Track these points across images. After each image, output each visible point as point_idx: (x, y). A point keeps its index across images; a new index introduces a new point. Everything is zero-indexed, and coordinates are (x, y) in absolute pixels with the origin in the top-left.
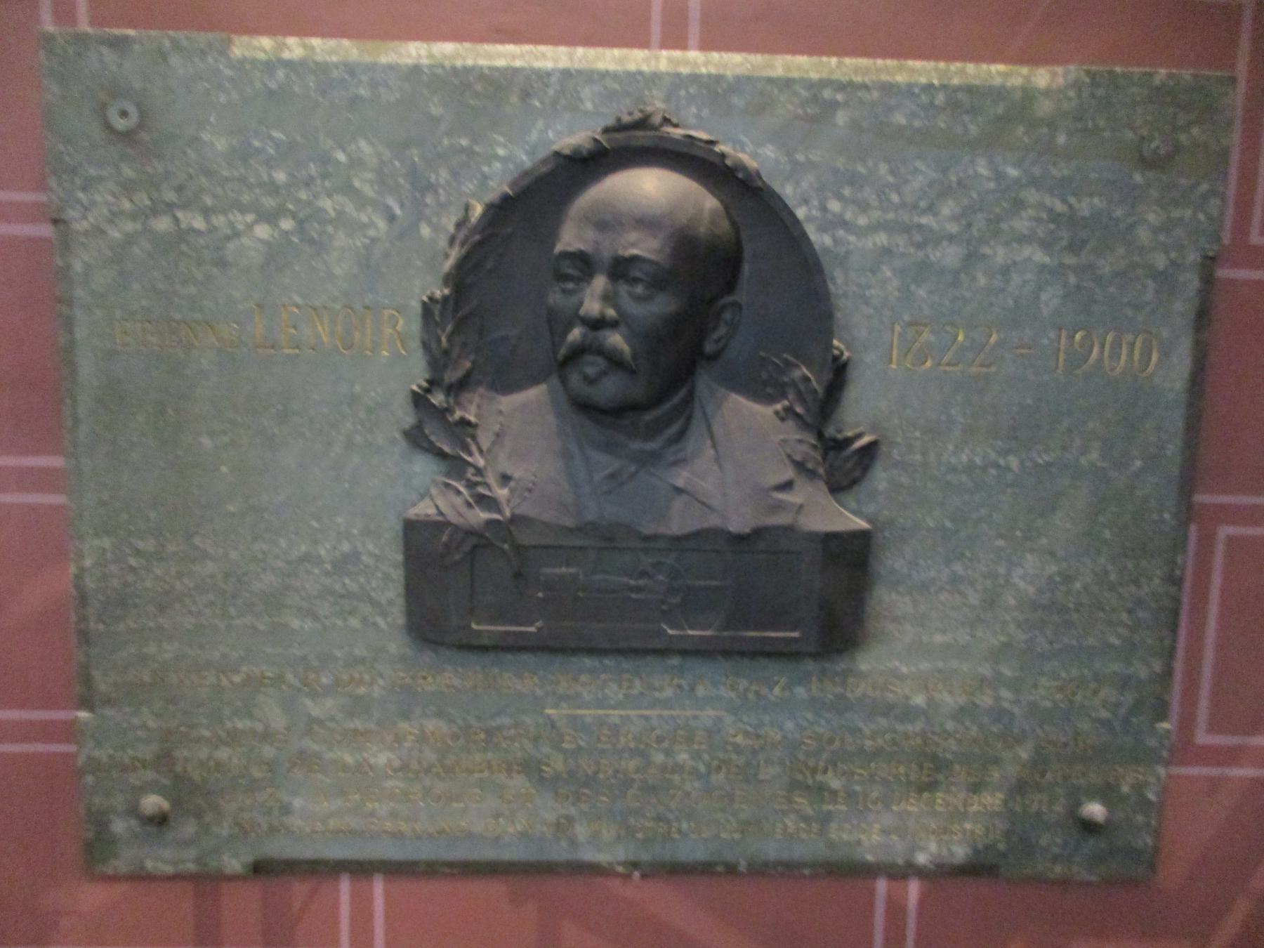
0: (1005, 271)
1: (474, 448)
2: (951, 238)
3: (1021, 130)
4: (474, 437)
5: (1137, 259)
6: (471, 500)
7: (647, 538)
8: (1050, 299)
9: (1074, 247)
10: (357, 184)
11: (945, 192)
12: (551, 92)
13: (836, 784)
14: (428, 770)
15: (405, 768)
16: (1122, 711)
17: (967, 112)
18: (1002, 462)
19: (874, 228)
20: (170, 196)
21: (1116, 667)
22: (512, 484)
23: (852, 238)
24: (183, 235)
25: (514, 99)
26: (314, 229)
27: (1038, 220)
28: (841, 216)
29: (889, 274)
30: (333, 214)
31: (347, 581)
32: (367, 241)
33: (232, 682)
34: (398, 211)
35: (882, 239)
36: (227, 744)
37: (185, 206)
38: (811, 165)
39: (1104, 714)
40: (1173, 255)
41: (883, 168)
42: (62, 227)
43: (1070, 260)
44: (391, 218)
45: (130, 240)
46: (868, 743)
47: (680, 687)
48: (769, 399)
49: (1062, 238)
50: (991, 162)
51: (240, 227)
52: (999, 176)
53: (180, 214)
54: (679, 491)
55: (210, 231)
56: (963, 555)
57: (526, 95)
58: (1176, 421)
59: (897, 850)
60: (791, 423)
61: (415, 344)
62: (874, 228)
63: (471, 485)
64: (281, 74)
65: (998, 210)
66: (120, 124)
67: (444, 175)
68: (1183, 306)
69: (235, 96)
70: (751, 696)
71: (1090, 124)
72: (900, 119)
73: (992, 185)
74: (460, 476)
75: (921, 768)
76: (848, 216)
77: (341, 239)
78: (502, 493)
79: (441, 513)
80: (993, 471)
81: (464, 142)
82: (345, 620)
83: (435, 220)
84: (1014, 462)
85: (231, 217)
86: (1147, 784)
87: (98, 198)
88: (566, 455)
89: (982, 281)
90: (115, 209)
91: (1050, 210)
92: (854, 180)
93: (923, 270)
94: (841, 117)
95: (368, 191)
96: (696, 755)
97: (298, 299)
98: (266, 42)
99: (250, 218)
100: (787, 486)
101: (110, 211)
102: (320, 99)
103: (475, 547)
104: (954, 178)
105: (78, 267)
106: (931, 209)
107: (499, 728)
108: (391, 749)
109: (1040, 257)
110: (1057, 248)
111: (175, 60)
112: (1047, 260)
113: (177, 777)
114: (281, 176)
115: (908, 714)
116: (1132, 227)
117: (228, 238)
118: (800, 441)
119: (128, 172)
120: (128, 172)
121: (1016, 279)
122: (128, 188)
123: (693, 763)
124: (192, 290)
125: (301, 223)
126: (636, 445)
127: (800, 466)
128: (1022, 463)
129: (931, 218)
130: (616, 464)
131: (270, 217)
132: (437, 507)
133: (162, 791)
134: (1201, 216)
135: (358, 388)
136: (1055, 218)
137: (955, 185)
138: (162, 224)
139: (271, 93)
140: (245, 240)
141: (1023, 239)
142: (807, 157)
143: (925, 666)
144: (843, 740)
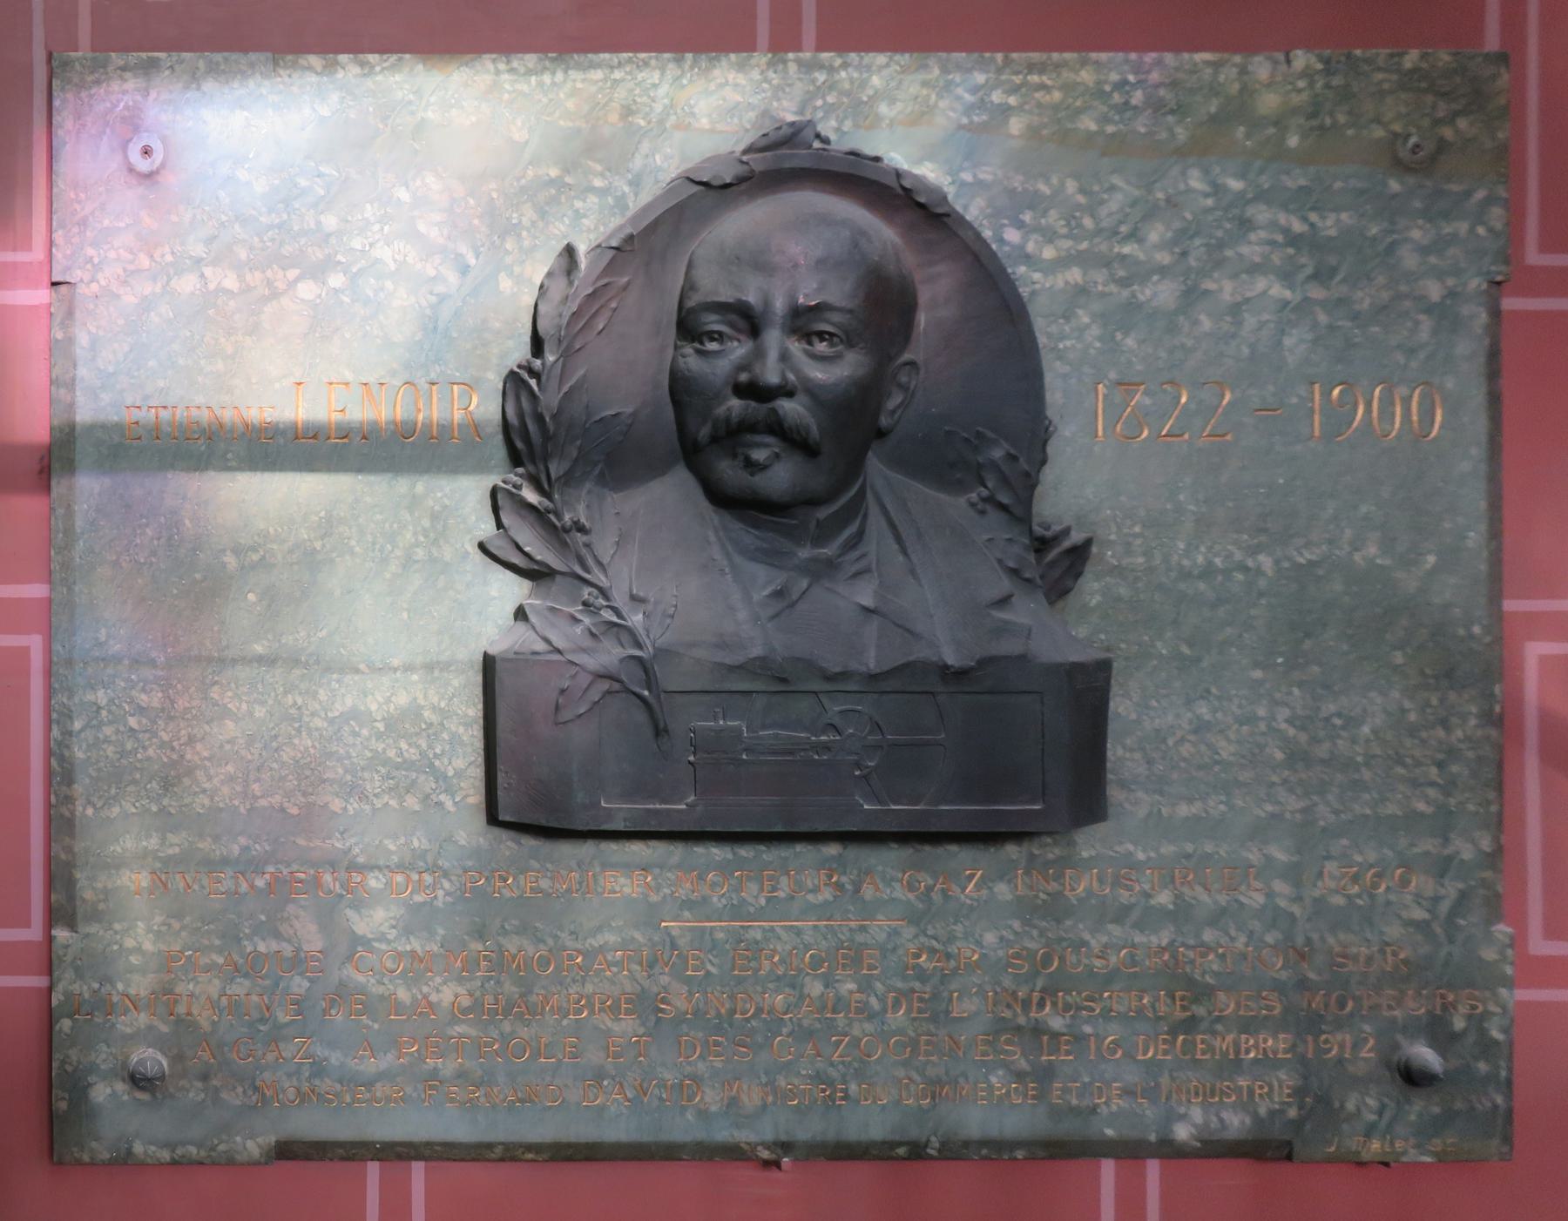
10: (422, 227)
34: (472, 262)
37: (215, 262)
44: (464, 270)
51: (281, 285)
53: (208, 271)
66: (143, 165)
85: (269, 273)
90: (131, 267)
99: (292, 274)
101: (125, 270)
102: (381, 126)
117: (266, 300)
124: (220, 366)
138: (187, 284)
140: (285, 301)
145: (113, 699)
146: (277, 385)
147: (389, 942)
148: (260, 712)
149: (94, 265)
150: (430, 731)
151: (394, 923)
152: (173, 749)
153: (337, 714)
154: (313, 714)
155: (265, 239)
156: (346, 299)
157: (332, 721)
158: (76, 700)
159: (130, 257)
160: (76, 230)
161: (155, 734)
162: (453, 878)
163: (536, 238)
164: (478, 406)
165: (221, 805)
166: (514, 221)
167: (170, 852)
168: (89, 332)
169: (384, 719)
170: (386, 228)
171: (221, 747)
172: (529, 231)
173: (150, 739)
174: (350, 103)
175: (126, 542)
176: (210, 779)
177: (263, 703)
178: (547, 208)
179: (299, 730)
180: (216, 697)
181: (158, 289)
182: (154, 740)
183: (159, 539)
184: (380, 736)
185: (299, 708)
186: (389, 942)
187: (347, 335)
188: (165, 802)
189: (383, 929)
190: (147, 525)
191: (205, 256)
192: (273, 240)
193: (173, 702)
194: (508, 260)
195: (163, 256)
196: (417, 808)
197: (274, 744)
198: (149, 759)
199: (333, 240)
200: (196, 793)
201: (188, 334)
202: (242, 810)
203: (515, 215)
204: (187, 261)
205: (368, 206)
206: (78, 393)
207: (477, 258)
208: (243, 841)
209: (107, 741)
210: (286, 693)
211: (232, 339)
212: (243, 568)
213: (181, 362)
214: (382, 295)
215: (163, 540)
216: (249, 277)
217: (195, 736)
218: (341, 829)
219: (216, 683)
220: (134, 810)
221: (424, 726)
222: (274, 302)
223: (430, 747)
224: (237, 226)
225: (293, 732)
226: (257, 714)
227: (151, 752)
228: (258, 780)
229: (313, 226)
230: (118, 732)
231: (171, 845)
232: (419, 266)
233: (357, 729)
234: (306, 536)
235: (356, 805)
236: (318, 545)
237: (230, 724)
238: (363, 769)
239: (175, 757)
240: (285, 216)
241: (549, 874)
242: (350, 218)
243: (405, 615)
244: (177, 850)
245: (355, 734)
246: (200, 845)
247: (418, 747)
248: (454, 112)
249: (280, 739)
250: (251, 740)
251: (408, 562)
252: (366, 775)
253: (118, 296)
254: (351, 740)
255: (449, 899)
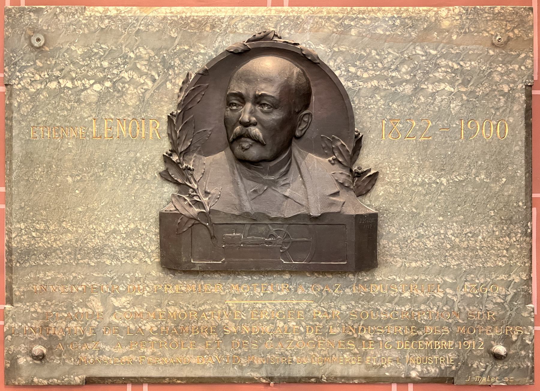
0: (433, 95)
1: (192, 180)
2: (407, 81)
3: (435, 34)
4: (192, 175)
5: (494, 87)
6: (190, 203)
7: (272, 219)
8: (455, 106)
9: (465, 83)
10: (139, 66)
11: (403, 62)
12: (224, 26)
13: (368, 337)
14: (169, 332)
15: (159, 330)
16: (509, 298)
17: (410, 27)
18: (438, 181)
19: (370, 79)
20: (58, 73)
21: (503, 277)
22: (210, 196)
23: (361, 83)
24: (62, 89)
25: (208, 29)
26: (120, 86)
27: (447, 72)
28: (356, 74)
29: (379, 98)
30: (128, 79)
31: (132, 242)
32: (143, 91)
33: (78, 290)
34: (157, 77)
35: (375, 83)
36: (75, 320)
37: (63, 78)
38: (341, 52)
39: (499, 300)
40: (511, 85)
41: (374, 53)
42: (9, 87)
43: (463, 89)
44: (154, 81)
45: (38, 92)
46: (383, 316)
47: (290, 289)
48: (327, 156)
49: (458, 80)
50: (423, 48)
51: (88, 86)
52: (427, 54)
53: (61, 81)
54: (287, 197)
55: (73, 88)
56: (423, 224)
57: (213, 27)
58: (521, 159)
59: (401, 370)
60: (337, 166)
61: (165, 135)
62: (370, 79)
63: (191, 196)
64: (107, 21)
65: (427, 69)
66: (37, 44)
67: (177, 62)
68: (519, 108)
69: (86, 31)
70: (324, 294)
71: (467, 31)
72: (380, 31)
73: (424, 58)
74: (186, 193)
75: (410, 329)
76: (359, 73)
77: (132, 90)
78: (205, 200)
79: (177, 210)
80: (434, 185)
81: (186, 48)
82: (132, 260)
83: (173, 81)
84: (444, 180)
85: (83, 82)
86: (524, 335)
87: (26, 75)
88: (235, 182)
89: (423, 99)
90: (33, 79)
91: (452, 68)
92: (361, 58)
93: (394, 96)
94: (353, 32)
95: (144, 69)
96: (299, 323)
97: (113, 117)
98: (101, 9)
99: (92, 82)
100: (336, 194)
101: (31, 80)
102: (123, 31)
103: (193, 225)
104: (406, 56)
105: (16, 104)
106: (397, 69)
107: (204, 311)
108: (153, 321)
109: (449, 88)
110: (457, 84)
111: (61, 17)
112: (452, 90)
113: (51, 336)
114: (106, 64)
115: (402, 301)
116: (490, 74)
117: (83, 90)
118: (341, 173)
119: (39, 64)
120: (39, 64)
121: (439, 99)
122: (39, 70)
123: (298, 327)
124: (66, 113)
125: (114, 83)
126: (266, 177)
127: (342, 184)
128: (448, 181)
129: (397, 73)
130: (257, 186)
131: (101, 81)
132: (175, 207)
133: (44, 344)
134: (523, 68)
135: (138, 155)
136: (454, 71)
137: (406, 58)
138: (53, 85)
139: (102, 29)
140: (89, 91)
141: (440, 81)
142: (339, 49)
143: (408, 278)
144: (370, 315)
145: (27, 227)
146: (86, 120)
147: (127, 309)
148: (80, 230)
149: (19, 78)
150: (142, 237)
151: (129, 302)
152: (49, 243)
153: (108, 231)
154: (99, 231)
155: (82, 70)
156: (111, 91)
157: (106, 234)
158: (13, 227)
159: (33, 76)
160: (12, 66)
161: (42, 238)
162: (150, 287)
163: (180, 70)
164: (159, 127)
165: (66, 262)
166: (172, 64)
167: (48, 278)
168: (17, 101)
169: (125, 233)
170: (126, 66)
171: (66, 242)
172: (178, 68)
173: (40, 240)
174: (112, 24)
175: (31, 173)
176: (62, 253)
177: (81, 228)
178: (184, 60)
179: (94, 237)
180: (64, 225)
181: (43, 87)
182: (42, 240)
183: (43, 172)
184: (124, 239)
185: (94, 229)
186: (127, 309)
187: (112, 103)
188: (46, 261)
189: (124, 304)
190: (39, 167)
191: (60, 75)
192: (84, 70)
193: (48, 227)
194: (170, 77)
195: (44, 75)
196: (137, 263)
197: (85, 242)
198: (40, 247)
199: (106, 70)
200: (57, 258)
201: (54, 102)
202: (74, 264)
203: (172, 62)
204: (53, 77)
205: (119, 59)
206: (13, 122)
207: (159, 77)
208: (74, 274)
209: (24, 240)
210: (89, 224)
211: (70, 104)
212: (74, 182)
213: (51, 112)
214: (124, 89)
215: (45, 172)
216: (76, 83)
217: (57, 239)
218: (110, 270)
219: (64, 221)
220: (34, 264)
221: (140, 235)
222: (85, 92)
223: (142, 242)
224: (71, 65)
225: (92, 238)
226: (79, 231)
227: (40, 244)
228: (79, 254)
229: (99, 65)
230: (28, 237)
231: (48, 276)
232: (138, 79)
233: (116, 236)
234: (97, 171)
235: (115, 262)
236: (101, 174)
237: (69, 235)
238: (118, 250)
239: (49, 246)
240: (89, 62)
241: (185, 285)
242: (112, 63)
243: (133, 198)
244: (50, 278)
245: (115, 238)
246: (59, 276)
247: (138, 242)
248: (150, 27)
249: (87, 240)
250: (77, 241)
251: (134, 180)
252: (119, 252)
253: (28, 89)
254: (113, 240)
255: (149, 294)
